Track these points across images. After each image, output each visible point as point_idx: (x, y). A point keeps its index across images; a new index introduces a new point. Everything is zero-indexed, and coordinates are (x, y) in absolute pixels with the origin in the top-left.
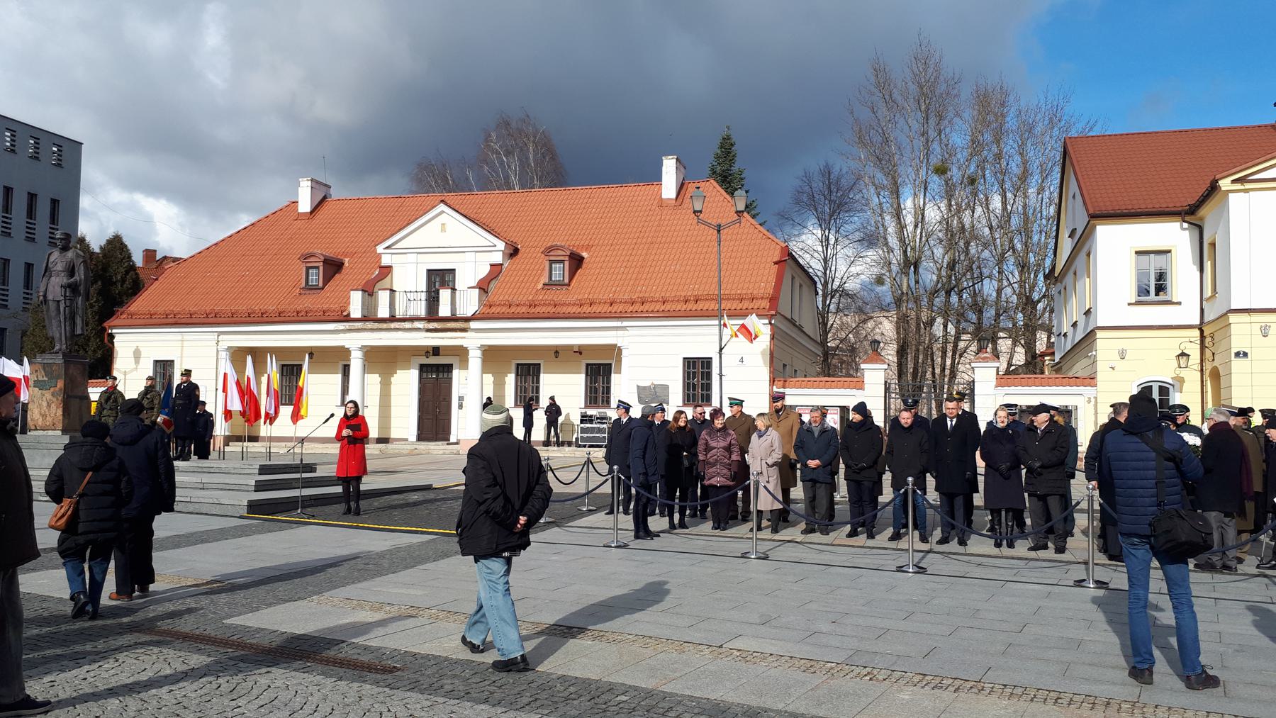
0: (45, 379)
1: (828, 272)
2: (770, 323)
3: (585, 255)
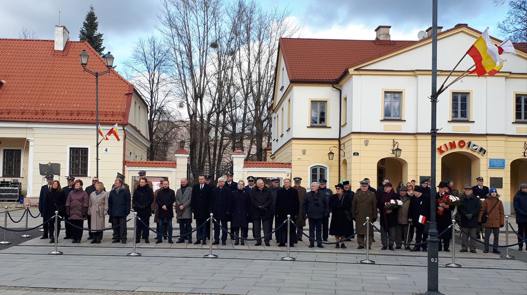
1: (153, 100)
2: (124, 129)
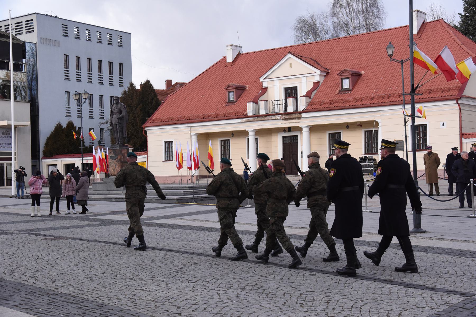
0: (114, 155)
2: (457, 103)
3: (363, 72)
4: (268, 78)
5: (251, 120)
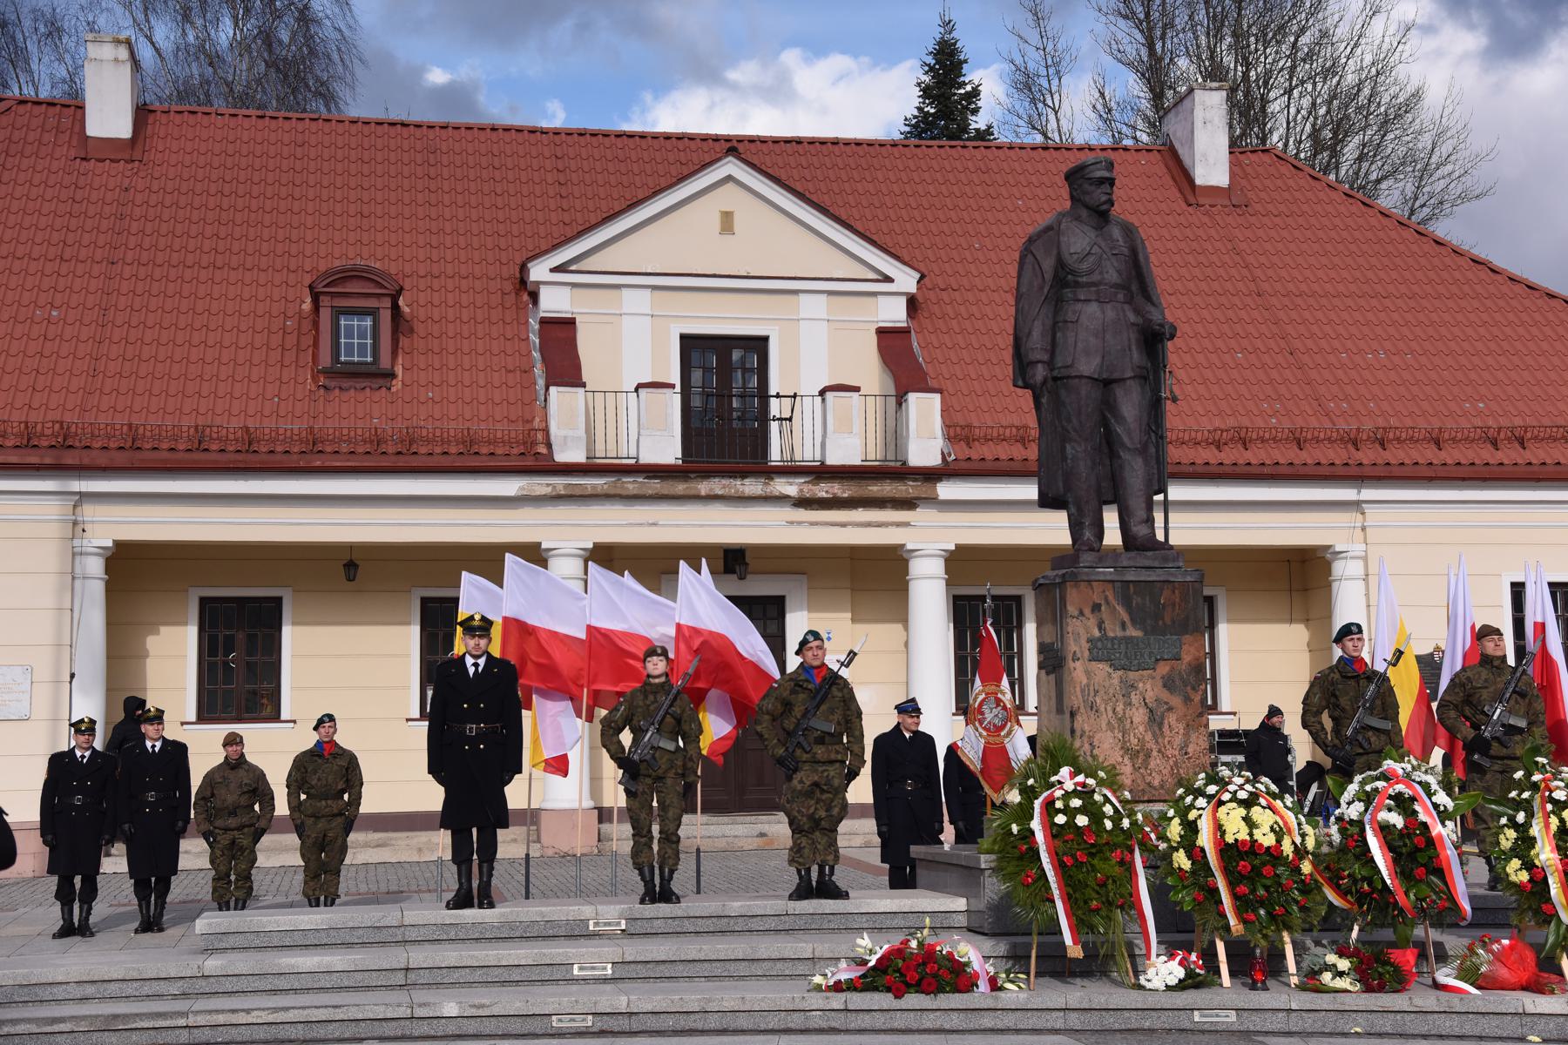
0: (1133, 632)
4: (573, 268)
5: (599, 491)
